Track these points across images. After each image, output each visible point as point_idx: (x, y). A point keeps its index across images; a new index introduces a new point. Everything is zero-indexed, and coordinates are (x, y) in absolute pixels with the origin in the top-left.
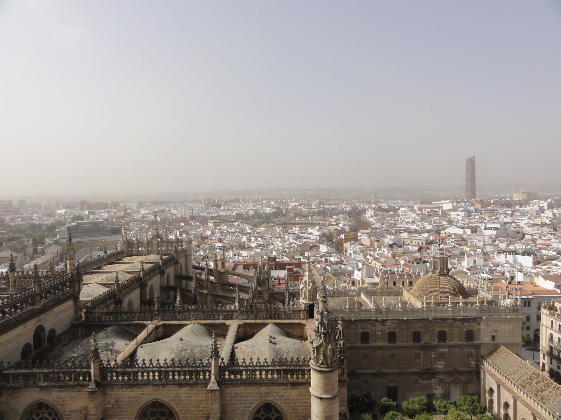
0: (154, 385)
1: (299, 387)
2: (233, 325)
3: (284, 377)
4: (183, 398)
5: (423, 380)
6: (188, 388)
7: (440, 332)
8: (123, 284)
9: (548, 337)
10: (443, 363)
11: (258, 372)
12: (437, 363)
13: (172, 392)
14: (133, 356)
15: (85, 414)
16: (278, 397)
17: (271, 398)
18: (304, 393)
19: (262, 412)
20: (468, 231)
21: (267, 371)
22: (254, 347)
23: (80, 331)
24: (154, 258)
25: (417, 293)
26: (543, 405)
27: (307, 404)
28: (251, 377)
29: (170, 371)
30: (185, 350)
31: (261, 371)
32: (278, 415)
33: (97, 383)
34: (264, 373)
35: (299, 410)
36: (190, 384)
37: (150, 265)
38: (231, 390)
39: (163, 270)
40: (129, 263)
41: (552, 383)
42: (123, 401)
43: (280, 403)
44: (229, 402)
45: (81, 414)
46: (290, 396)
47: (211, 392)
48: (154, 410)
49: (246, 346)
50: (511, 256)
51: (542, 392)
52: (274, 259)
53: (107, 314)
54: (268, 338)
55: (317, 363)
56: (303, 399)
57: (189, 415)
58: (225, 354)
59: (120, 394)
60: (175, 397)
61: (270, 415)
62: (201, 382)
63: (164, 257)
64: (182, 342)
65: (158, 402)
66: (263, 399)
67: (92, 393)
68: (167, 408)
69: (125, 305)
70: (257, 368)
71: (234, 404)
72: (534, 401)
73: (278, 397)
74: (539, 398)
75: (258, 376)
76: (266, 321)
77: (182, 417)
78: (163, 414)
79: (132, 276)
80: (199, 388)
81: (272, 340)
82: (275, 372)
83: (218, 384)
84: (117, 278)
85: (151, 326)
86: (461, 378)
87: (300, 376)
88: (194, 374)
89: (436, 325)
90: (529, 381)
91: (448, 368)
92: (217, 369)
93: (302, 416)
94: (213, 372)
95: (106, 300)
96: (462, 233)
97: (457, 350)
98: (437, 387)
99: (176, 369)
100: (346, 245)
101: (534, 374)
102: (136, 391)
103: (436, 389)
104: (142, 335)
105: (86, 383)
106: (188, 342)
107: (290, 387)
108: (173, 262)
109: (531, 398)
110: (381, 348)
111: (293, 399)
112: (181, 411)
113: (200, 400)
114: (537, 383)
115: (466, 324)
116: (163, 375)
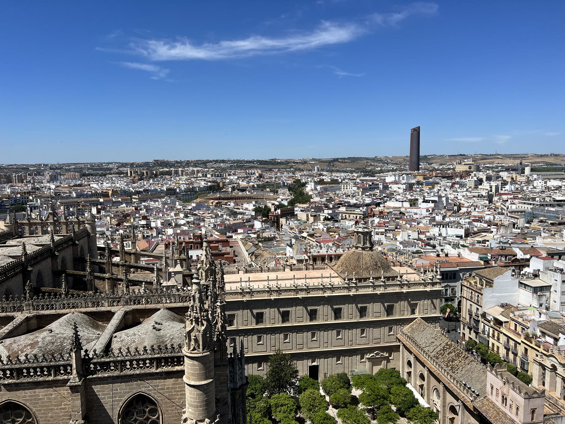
2: (119, 312)
4: (40, 397)
9: (468, 307)
11: (128, 363)
16: (151, 388)
17: (143, 390)
20: (407, 205)
22: (135, 335)
24: (46, 239)
25: (340, 269)
26: (453, 375)
29: (24, 368)
30: (53, 343)
31: (131, 361)
34: (135, 362)
35: (176, 398)
40: (16, 246)
41: (462, 353)
43: (154, 393)
46: (164, 385)
49: (127, 335)
50: (444, 229)
51: (452, 362)
54: (153, 324)
55: (189, 349)
60: (31, 396)
64: (51, 334)
66: (135, 391)
72: (445, 370)
73: (151, 388)
74: (450, 368)
76: (158, 306)
81: (157, 326)
85: (20, 317)
90: (442, 352)
92: (80, 363)
94: (74, 366)
96: (401, 206)
99: (30, 365)
100: (283, 221)
101: (447, 344)
106: (58, 334)
114: (448, 354)
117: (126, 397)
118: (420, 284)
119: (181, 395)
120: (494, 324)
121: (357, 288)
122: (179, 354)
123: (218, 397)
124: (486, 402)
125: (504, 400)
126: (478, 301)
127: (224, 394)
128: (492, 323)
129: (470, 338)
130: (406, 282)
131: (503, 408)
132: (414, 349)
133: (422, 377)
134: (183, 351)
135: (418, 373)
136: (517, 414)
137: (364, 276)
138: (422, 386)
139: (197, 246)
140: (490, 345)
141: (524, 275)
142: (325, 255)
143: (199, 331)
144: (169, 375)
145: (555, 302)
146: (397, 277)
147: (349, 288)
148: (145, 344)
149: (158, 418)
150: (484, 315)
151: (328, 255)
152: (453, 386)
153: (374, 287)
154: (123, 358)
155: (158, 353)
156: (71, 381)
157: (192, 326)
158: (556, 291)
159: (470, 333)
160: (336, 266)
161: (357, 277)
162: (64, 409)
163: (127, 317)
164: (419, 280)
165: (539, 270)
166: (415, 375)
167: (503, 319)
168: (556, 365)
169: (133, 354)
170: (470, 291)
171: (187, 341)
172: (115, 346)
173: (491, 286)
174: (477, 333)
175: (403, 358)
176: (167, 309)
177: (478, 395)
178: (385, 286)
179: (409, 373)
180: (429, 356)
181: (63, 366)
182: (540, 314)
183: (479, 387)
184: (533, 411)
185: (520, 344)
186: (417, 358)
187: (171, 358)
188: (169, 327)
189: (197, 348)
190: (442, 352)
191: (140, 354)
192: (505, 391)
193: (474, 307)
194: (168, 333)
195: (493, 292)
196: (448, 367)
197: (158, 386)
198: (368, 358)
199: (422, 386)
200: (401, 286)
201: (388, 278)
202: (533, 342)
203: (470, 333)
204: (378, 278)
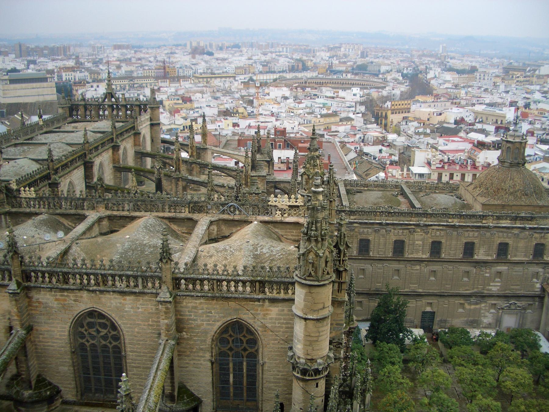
0: (88, 290)
1: (280, 304)
3: (260, 291)
4: (127, 309)
5: (470, 304)
6: (132, 297)
7: (500, 244)
8: (60, 160)
10: (499, 284)
12: (491, 284)
13: (112, 301)
14: (66, 252)
15: (9, 319)
18: (286, 312)
19: (231, 332)
21: (237, 282)
22: (225, 250)
23: (3, 220)
24: (105, 125)
27: (290, 326)
28: (216, 287)
29: (109, 275)
32: (252, 337)
33: (19, 284)
34: (233, 284)
35: (279, 331)
36: (135, 293)
37: (99, 135)
38: (188, 304)
39: (117, 143)
42: (52, 307)
44: (186, 318)
45: (5, 319)
47: (161, 304)
48: (92, 320)
52: (283, 132)
53: (35, 199)
56: (284, 319)
57: (136, 330)
58: (183, 256)
59: (48, 299)
61: (240, 336)
62: (149, 291)
63: (118, 125)
65: (96, 311)
67: (14, 294)
68: (108, 319)
69: (64, 187)
70: (224, 277)
71: (194, 320)
75: (225, 288)
77: (127, 331)
78: (104, 326)
79: (70, 149)
80: (146, 298)
82: (247, 284)
83: (171, 295)
84: (50, 151)
85: (92, 216)
86: (519, 304)
87: (282, 291)
88: (140, 280)
89: (497, 235)
91: (506, 290)
93: (283, 340)
95: (36, 181)
97: (519, 269)
98: (487, 314)
102: (67, 296)
103: (485, 316)
104: (81, 228)
105: (6, 282)
107: (267, 303)
108: (133, 132)
110: (420, 261)
111: (271, 319)
112: (124, 324)
113: (149, 313)
115: (536, 235)
116: (100, 279)
139: (280, 145)
149: (257, 351)
156: (161, 295)
162: (151, 325)
163: (211, 228)
172: (201, 262)
176: (261, 222)
181: (152, 277)
191: (238, 275)
194: (267, 252)
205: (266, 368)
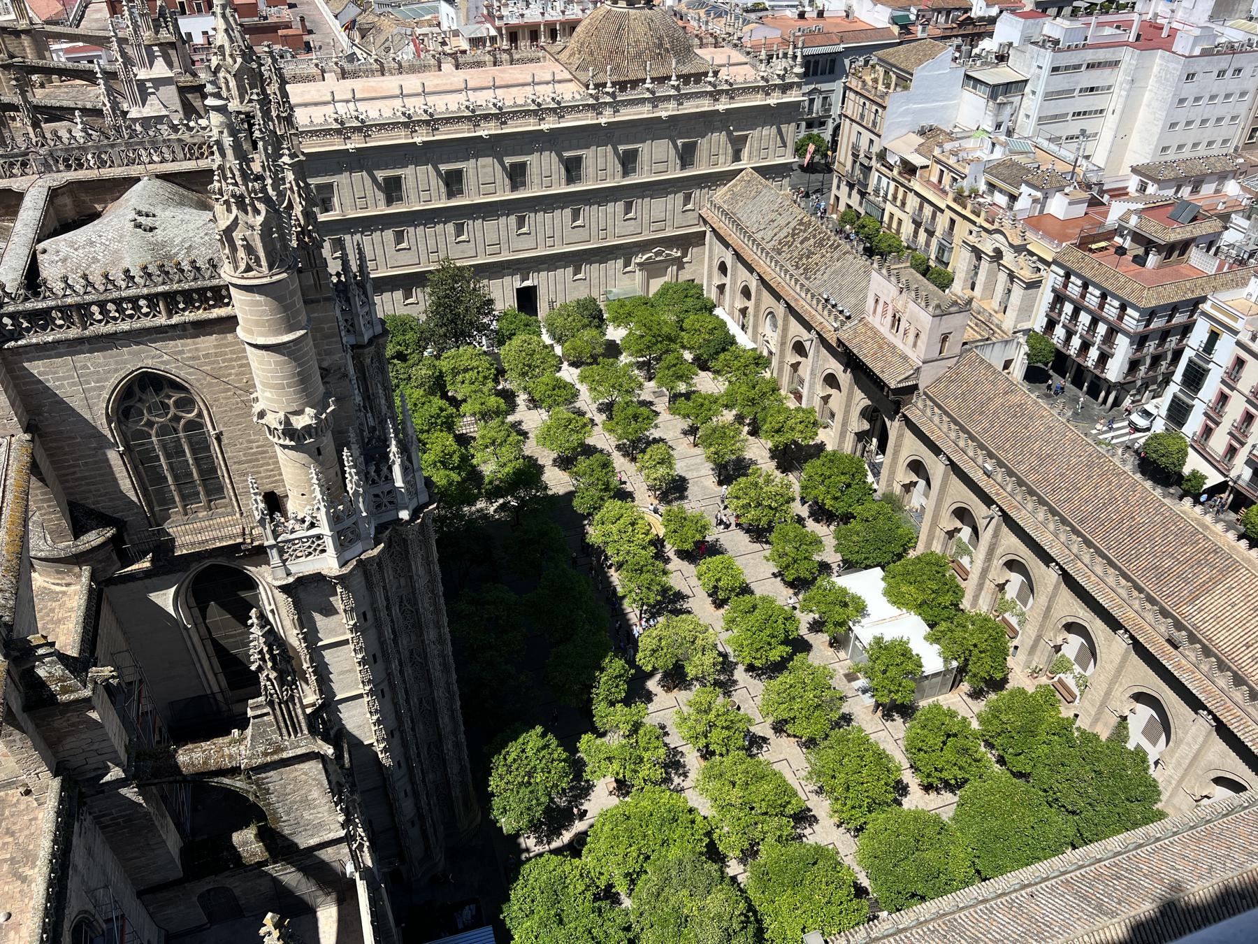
9: (853, 139)
16: (166, 357)
17: (150, 362)
22: (92, 243)
25: (576, 61)
26: (806, 283)
31: (102, 305)
35: (230, 374)
46: (197, 349)
49: (71, 244)
51: (808, 257)
54: (133, 215)
55: (236, 268)
56: (232, 352)
72: (792, 276)
73: (166, 357)
74: (801, 271)
81: (141, 219)
90: (789, 238)
101: (801, 223)
109: (786, 271)
114: (802, 243)
117: (113, 381)
118: (756, 89)
119: (241, 366)
120: (900, 173)
121: (616, 106)
122: (215, 282)
123: (325, 365)
124: (861, 329)
125: (896, 321)
126: (874, 124)
127: (337, 357)
128: (895, 172)
129: (849, 206)
130: (726, 87)
131: (891, 338)
132: (734, 238)
133: (746, 293)
134: (223, 275)
135: (740, 286)
136: (915, 345)
137: (632, 77)
138: (744, 311)
140: (886, 218)
141: (979, 56)
142: (538, 25)
143: (253, 228)
144: (201, 328)
145: (1028, 116)
146: (706, 74)
147: (597, 108)
148: (126, 263)
149: (200, 415)
150: (882, 156)
151: (547, 24)
152: (804, 305)
153: (655, 101)
154: (78, 299)
155: (164, 283)
157: (232, 217)
158: (1034, 93)
159: (850, 196)
160: (567, 52)
161: (615, 78)
164: (756, 80)
165: (1010, 44)
166: (733, 291)
167: (917, 160)
168: (1002, 248)
169: (102, 288)
170: (862, 101)
171: (227, 251)
172: (50, 272)
173: (906, 88)
174: (863, 194)
175: (711, 258)
176: (158, 177)
177: (848, 318)
178: (680, 99)
179: (721, 288)
180: (763, 249)
182: (994, 145)
183: (853, 301)
184: (945, 338)
185: (942, 211)
186: (737, 255)
187: (197, 290)
188: (174, 222)
189: (254, 266)
190: (789, 238)
191: (119, 288)
192: (899, 307)
193: (867, 135)
195: (908, 101)
196: (797, 267)
197: (182, 352)
198: (639, 264)
199: (744, 311)
200: (715, 95)
201: (686, 79)
202: (969, 207)
203: (850, 196)
204: (662, 80)
205: (225, 441)
